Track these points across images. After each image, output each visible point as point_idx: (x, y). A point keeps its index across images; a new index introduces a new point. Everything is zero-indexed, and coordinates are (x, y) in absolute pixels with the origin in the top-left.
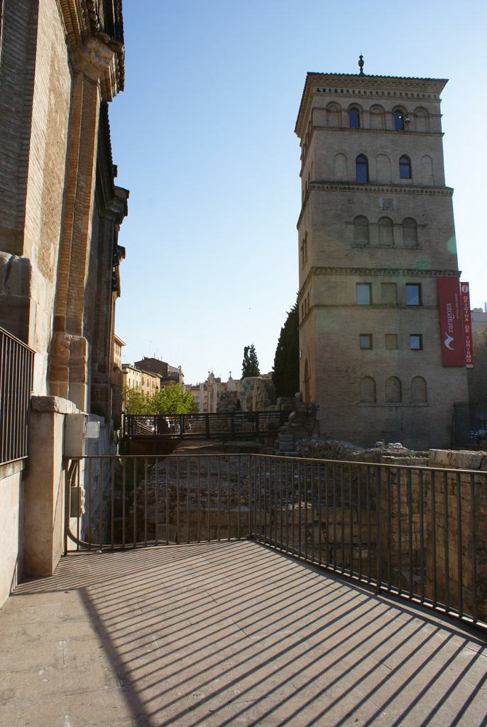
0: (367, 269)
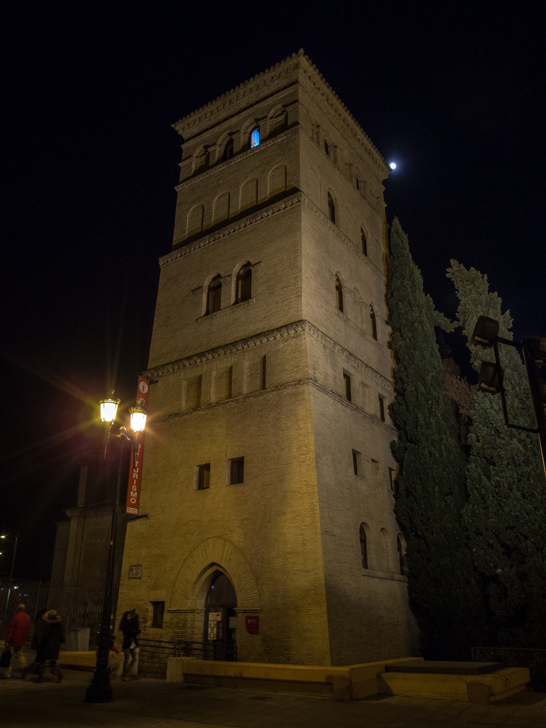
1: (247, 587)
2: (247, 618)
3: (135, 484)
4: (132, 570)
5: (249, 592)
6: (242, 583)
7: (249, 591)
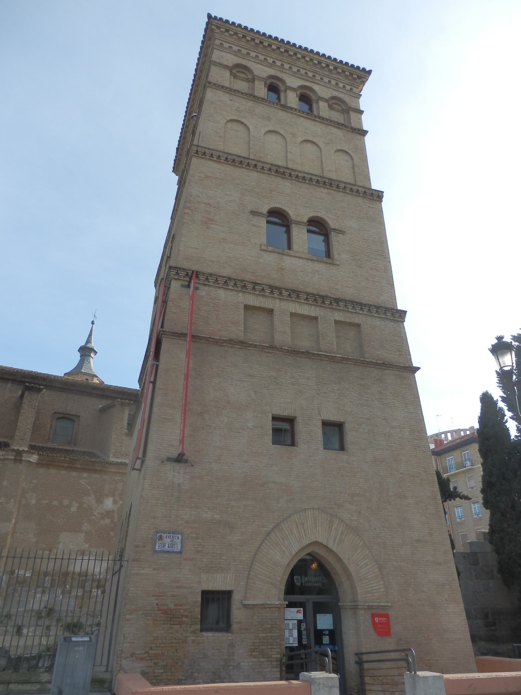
1: (369, 577)
2: (374, 616)
4: (161, 538)
5: (373, 583)
6: (362, 571)
7: (372, 582)
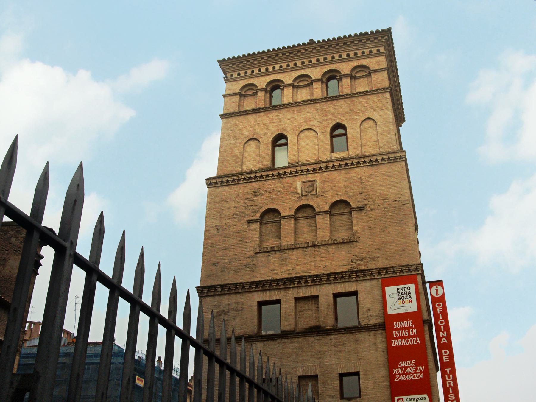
0: (273, 281)
3: (451, 392)
